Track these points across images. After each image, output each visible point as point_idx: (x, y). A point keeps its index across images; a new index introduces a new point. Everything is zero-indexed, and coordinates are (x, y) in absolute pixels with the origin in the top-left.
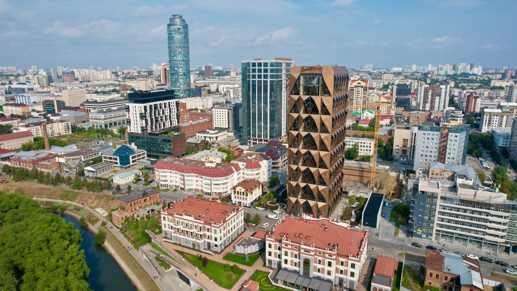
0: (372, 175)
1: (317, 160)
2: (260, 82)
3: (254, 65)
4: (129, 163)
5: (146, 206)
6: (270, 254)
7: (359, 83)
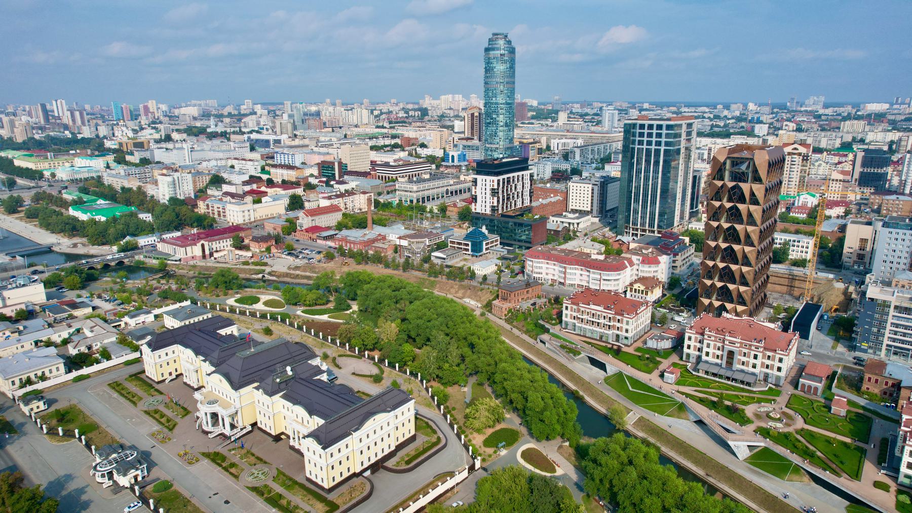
0: (807, 286)
1: (740, 256)
2: (648, 152)
3: (642, 127)
4: (481, 250)
5: (528, 298)
6: (689, 347)
7: (795, 149)
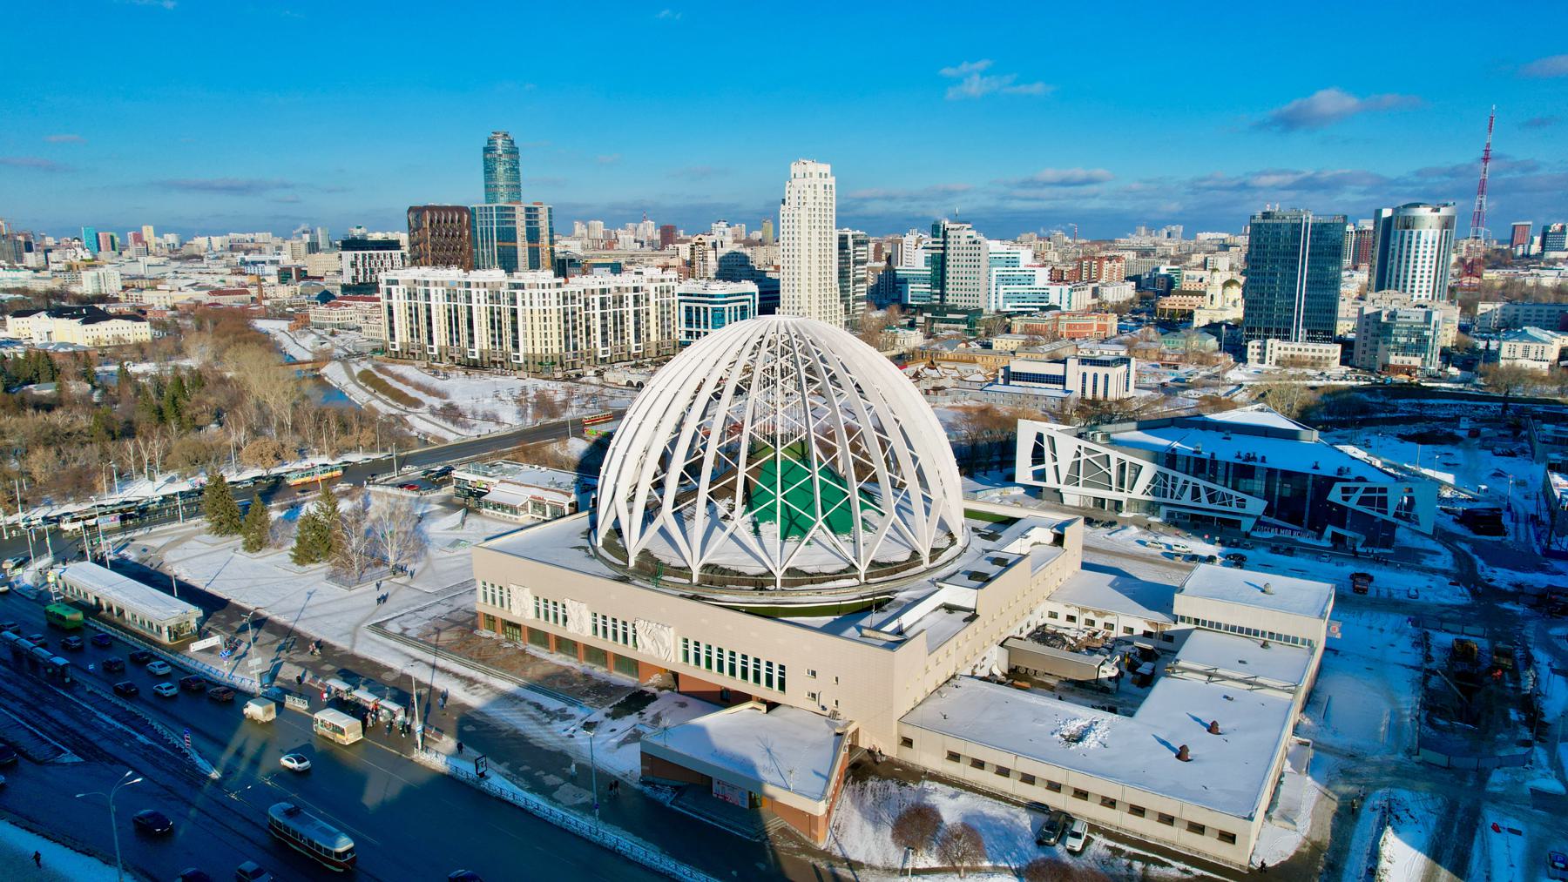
7: (700, 239)
